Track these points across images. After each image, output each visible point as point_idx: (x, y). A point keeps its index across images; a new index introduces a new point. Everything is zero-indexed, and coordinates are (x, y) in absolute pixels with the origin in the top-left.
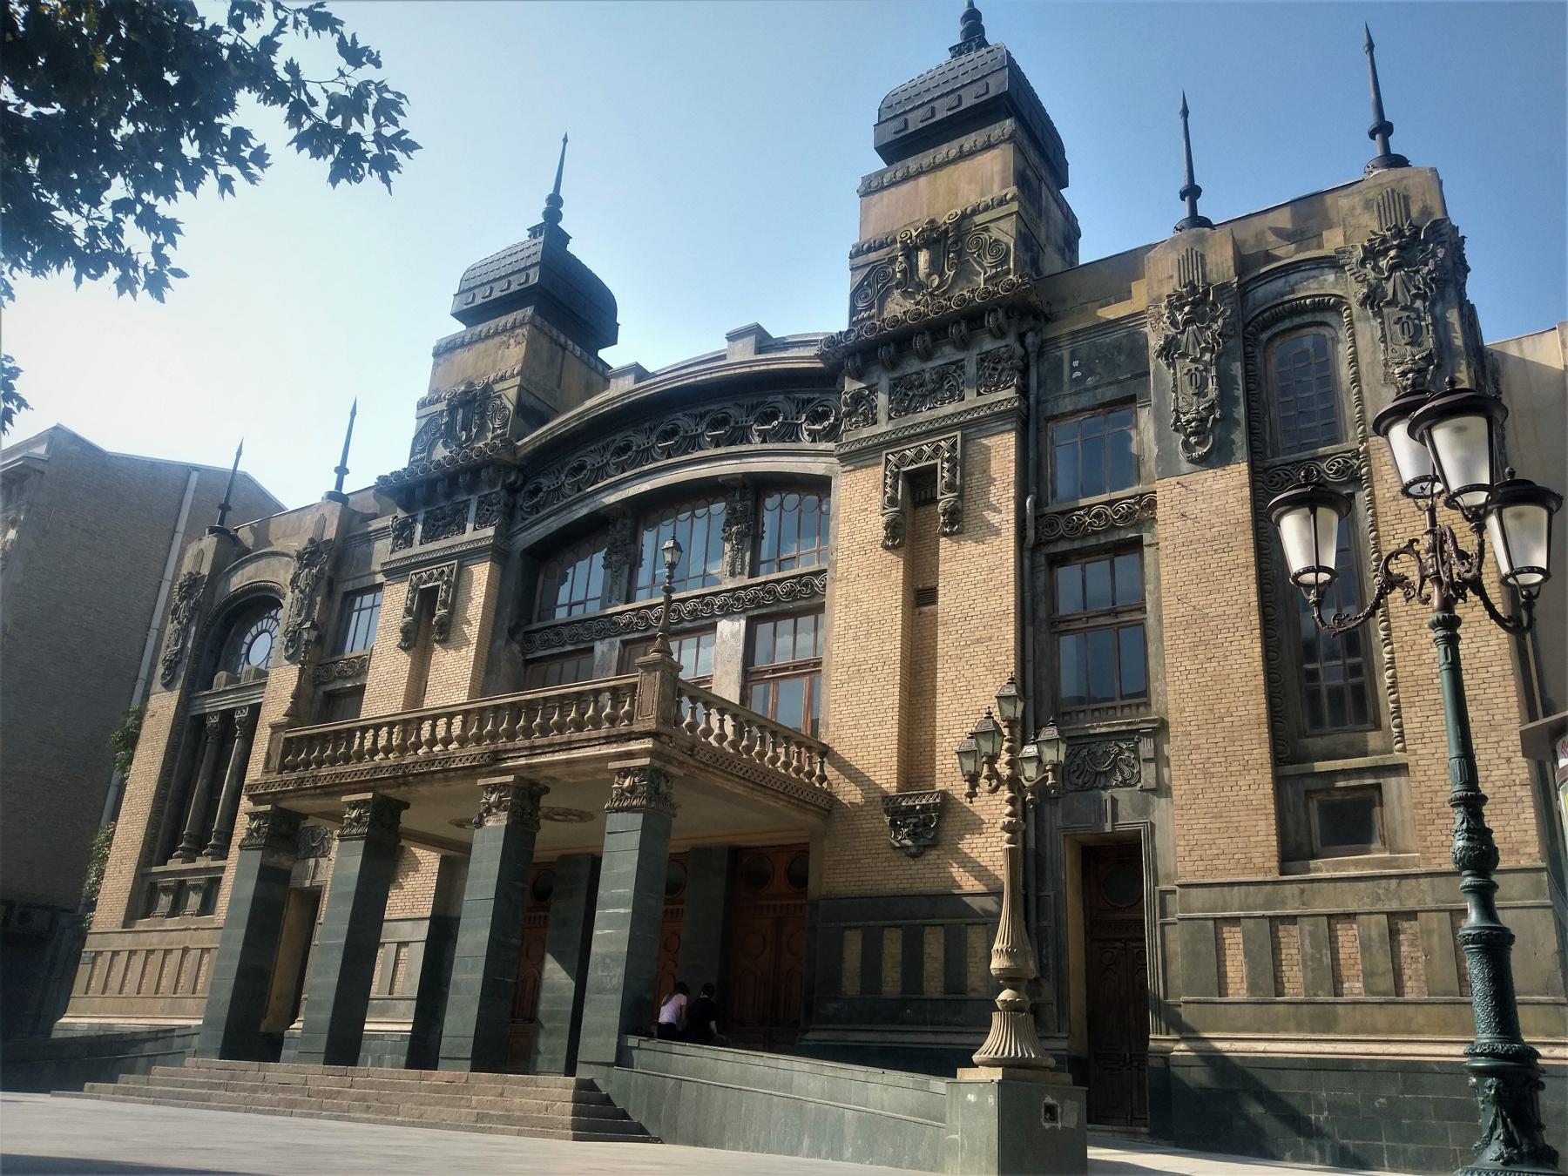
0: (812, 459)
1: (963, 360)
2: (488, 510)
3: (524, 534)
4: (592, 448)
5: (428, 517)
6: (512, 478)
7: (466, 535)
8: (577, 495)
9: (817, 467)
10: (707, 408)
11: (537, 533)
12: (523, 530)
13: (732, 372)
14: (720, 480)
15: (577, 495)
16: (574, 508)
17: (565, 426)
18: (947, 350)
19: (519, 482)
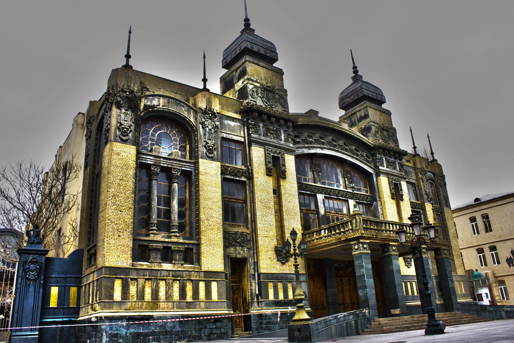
4: (311, 131)
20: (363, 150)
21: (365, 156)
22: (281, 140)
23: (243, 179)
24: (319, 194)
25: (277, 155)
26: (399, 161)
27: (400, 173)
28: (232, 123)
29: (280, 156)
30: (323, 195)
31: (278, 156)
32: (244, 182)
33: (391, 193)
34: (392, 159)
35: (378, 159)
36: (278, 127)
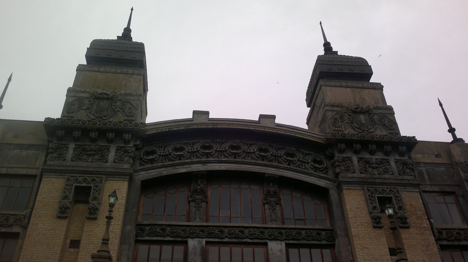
0: (317, 179)
1: (388, 159)
2: (123, 154)
3: (143, 173)
4: (186, 142)
5: (77, 148)
6: (138, 143)
7: (108, 164)
8: (178, 162)
9: (322, 183)
10: (254, 143)
11: (152, 174)
12: (142, 170)
13: (276, 131)
14: (266, 175)
15: (178, 162)
16: (177, 167)
17: (177, 127)
18: (380, 153)
19: (140, 146)
20: (306, 152)
21: (310, 161)
22: (107, 162)
23: (16, 229)
24: (193, 238)
25: (88, 185)
26: (398, 157)
27: (400, 177)
28: (24, 153)
29: (92, 185)
30: (204, 241)
31: (89, 185)
32: (16, 236)
33: (372, 218)
34: (377, 157)
35: (339, 162)
36: (107, 145)
